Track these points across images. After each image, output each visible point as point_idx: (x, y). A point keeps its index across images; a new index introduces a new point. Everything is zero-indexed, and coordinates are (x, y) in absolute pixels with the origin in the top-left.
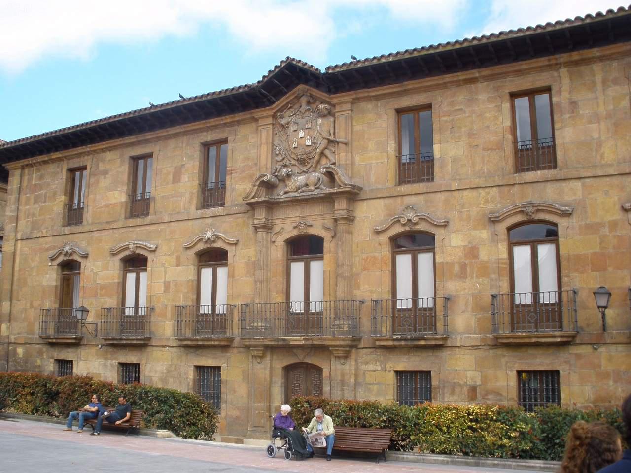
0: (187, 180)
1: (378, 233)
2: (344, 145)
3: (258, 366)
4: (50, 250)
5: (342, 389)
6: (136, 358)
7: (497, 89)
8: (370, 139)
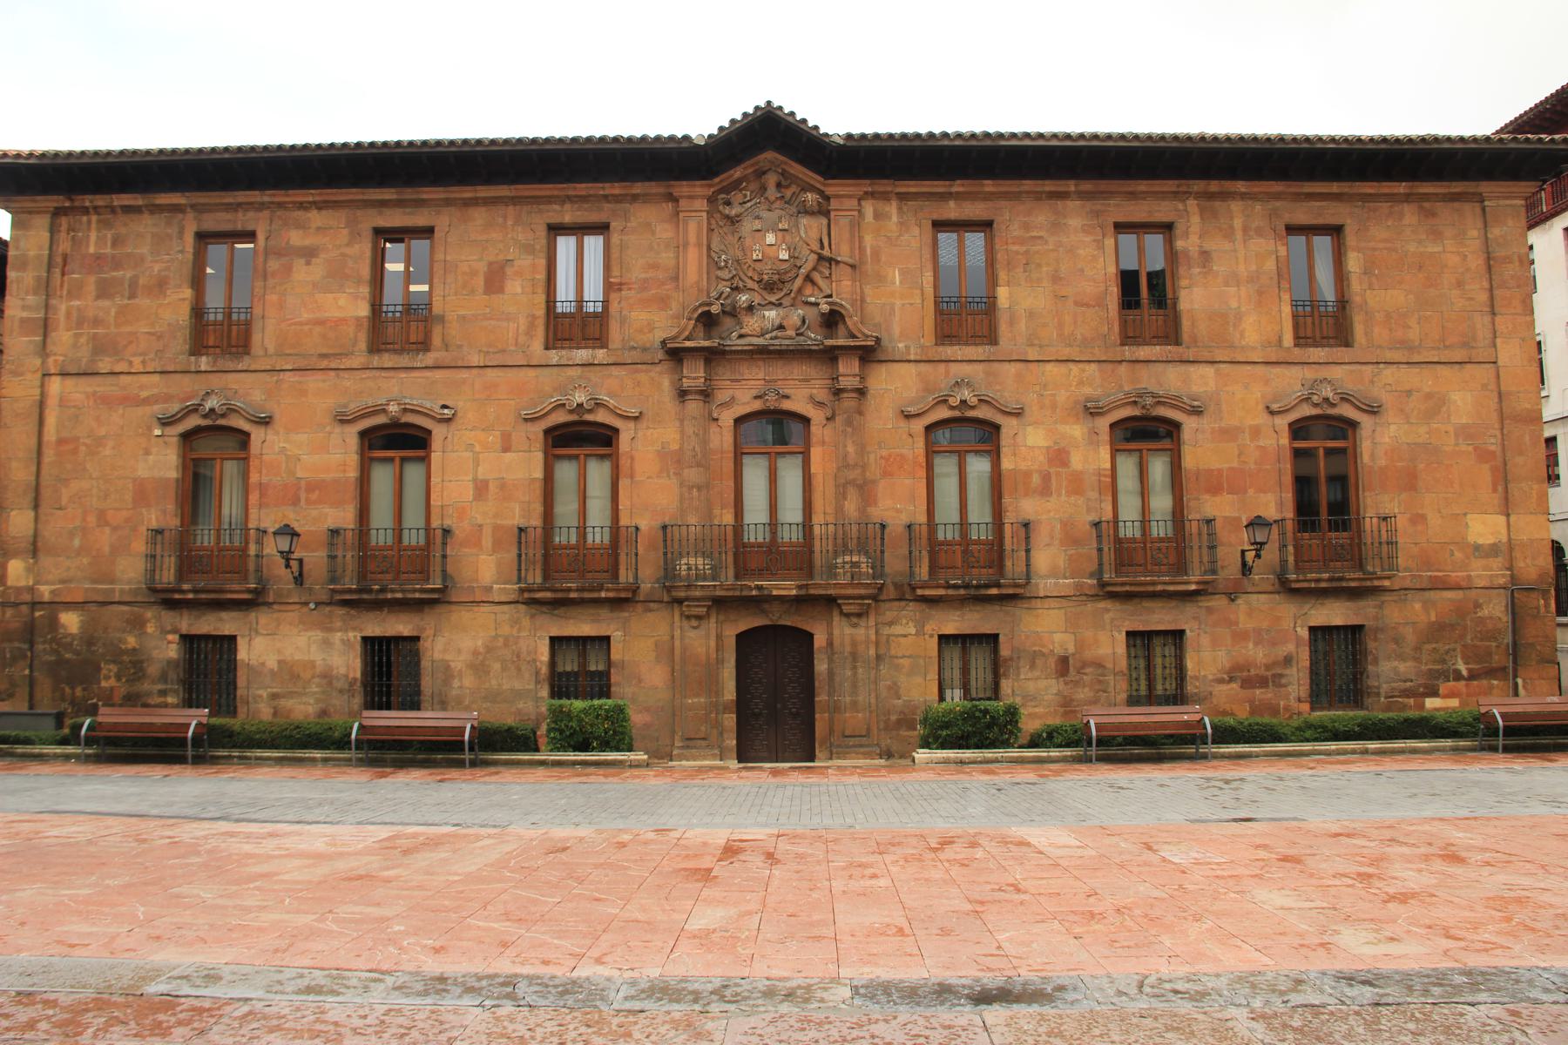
1: (908, 417)
2: (849, 269)
3: (692, 634)
4: (156, 402)
5: (854, 668)
6: (410, 627)
7: (1097, 214)
8: (893, 265)
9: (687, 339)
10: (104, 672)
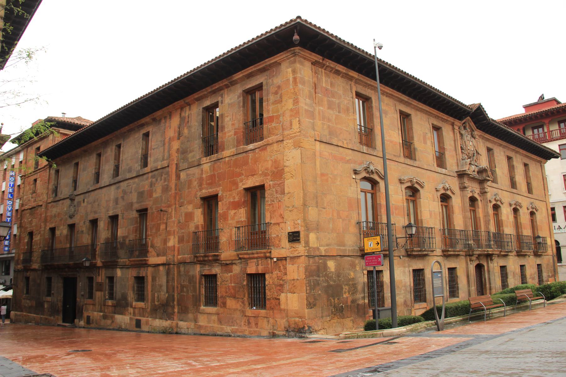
10: (344, 290)
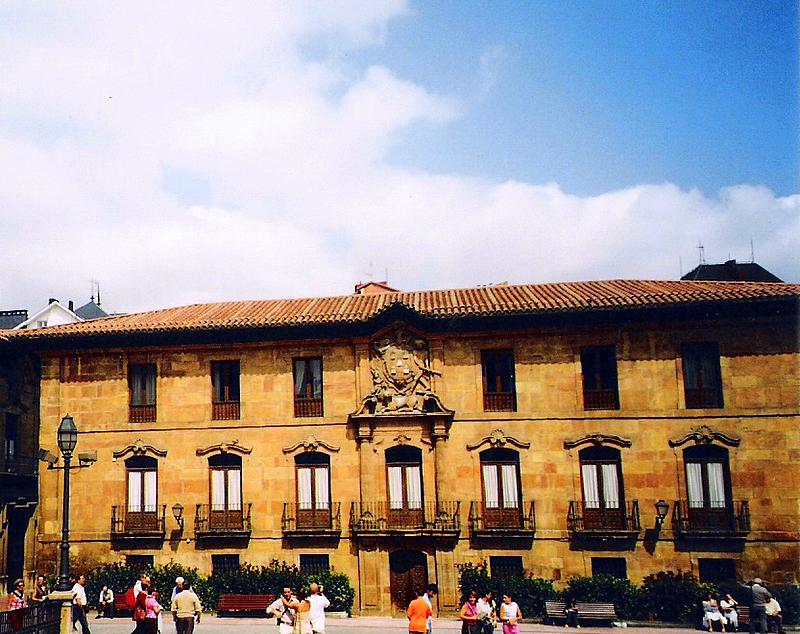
0: (280, 389)
1: (469, 449)
9: (362, 413)
